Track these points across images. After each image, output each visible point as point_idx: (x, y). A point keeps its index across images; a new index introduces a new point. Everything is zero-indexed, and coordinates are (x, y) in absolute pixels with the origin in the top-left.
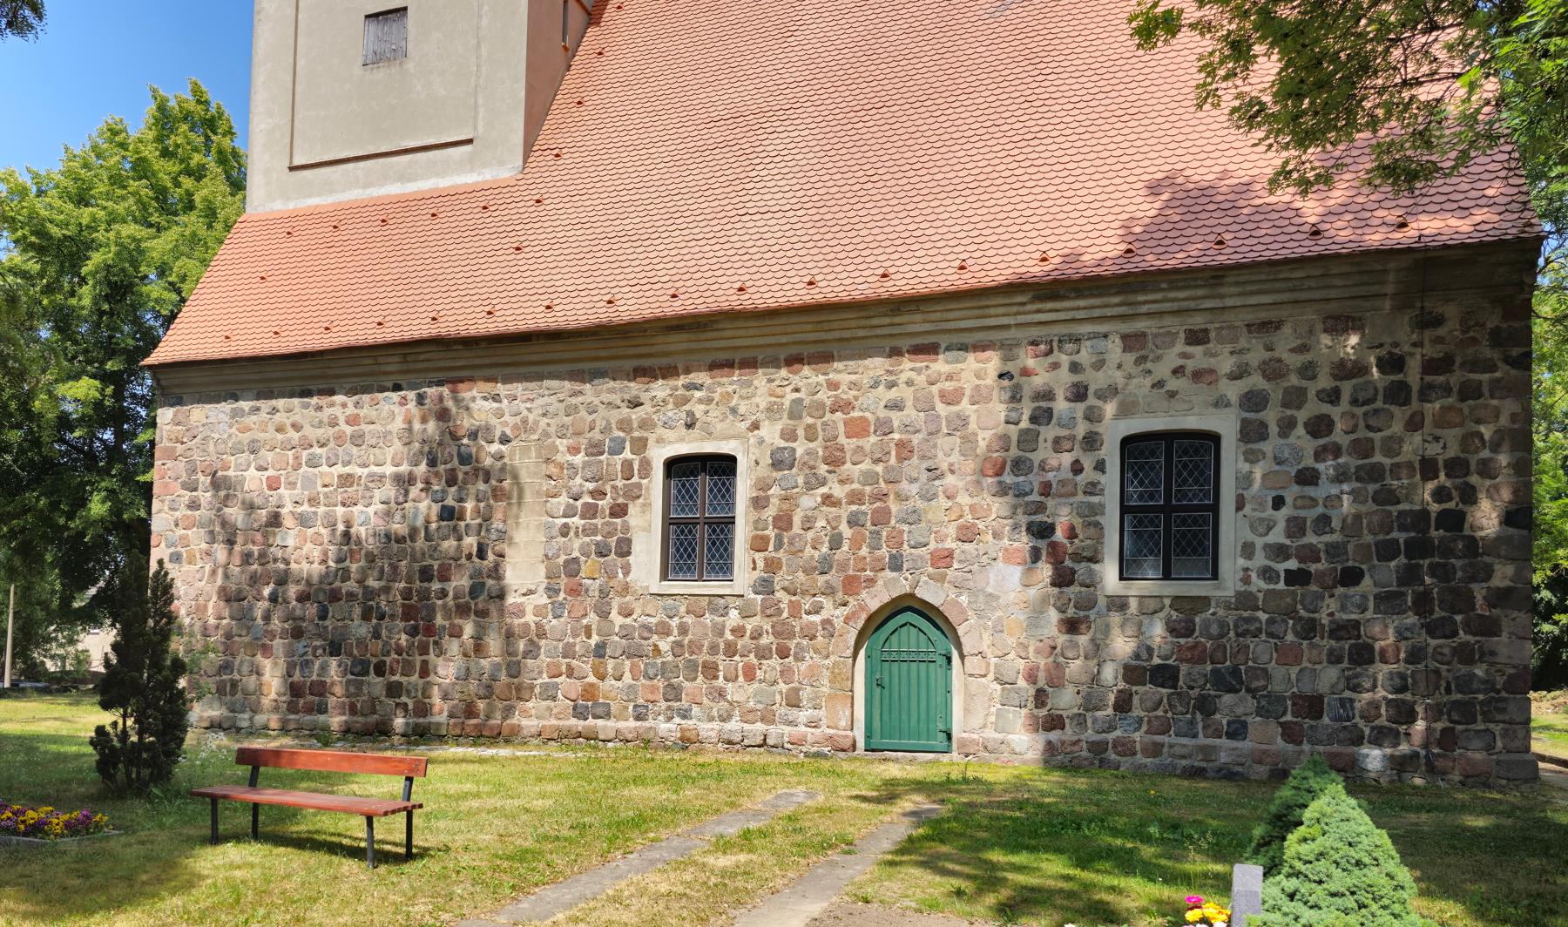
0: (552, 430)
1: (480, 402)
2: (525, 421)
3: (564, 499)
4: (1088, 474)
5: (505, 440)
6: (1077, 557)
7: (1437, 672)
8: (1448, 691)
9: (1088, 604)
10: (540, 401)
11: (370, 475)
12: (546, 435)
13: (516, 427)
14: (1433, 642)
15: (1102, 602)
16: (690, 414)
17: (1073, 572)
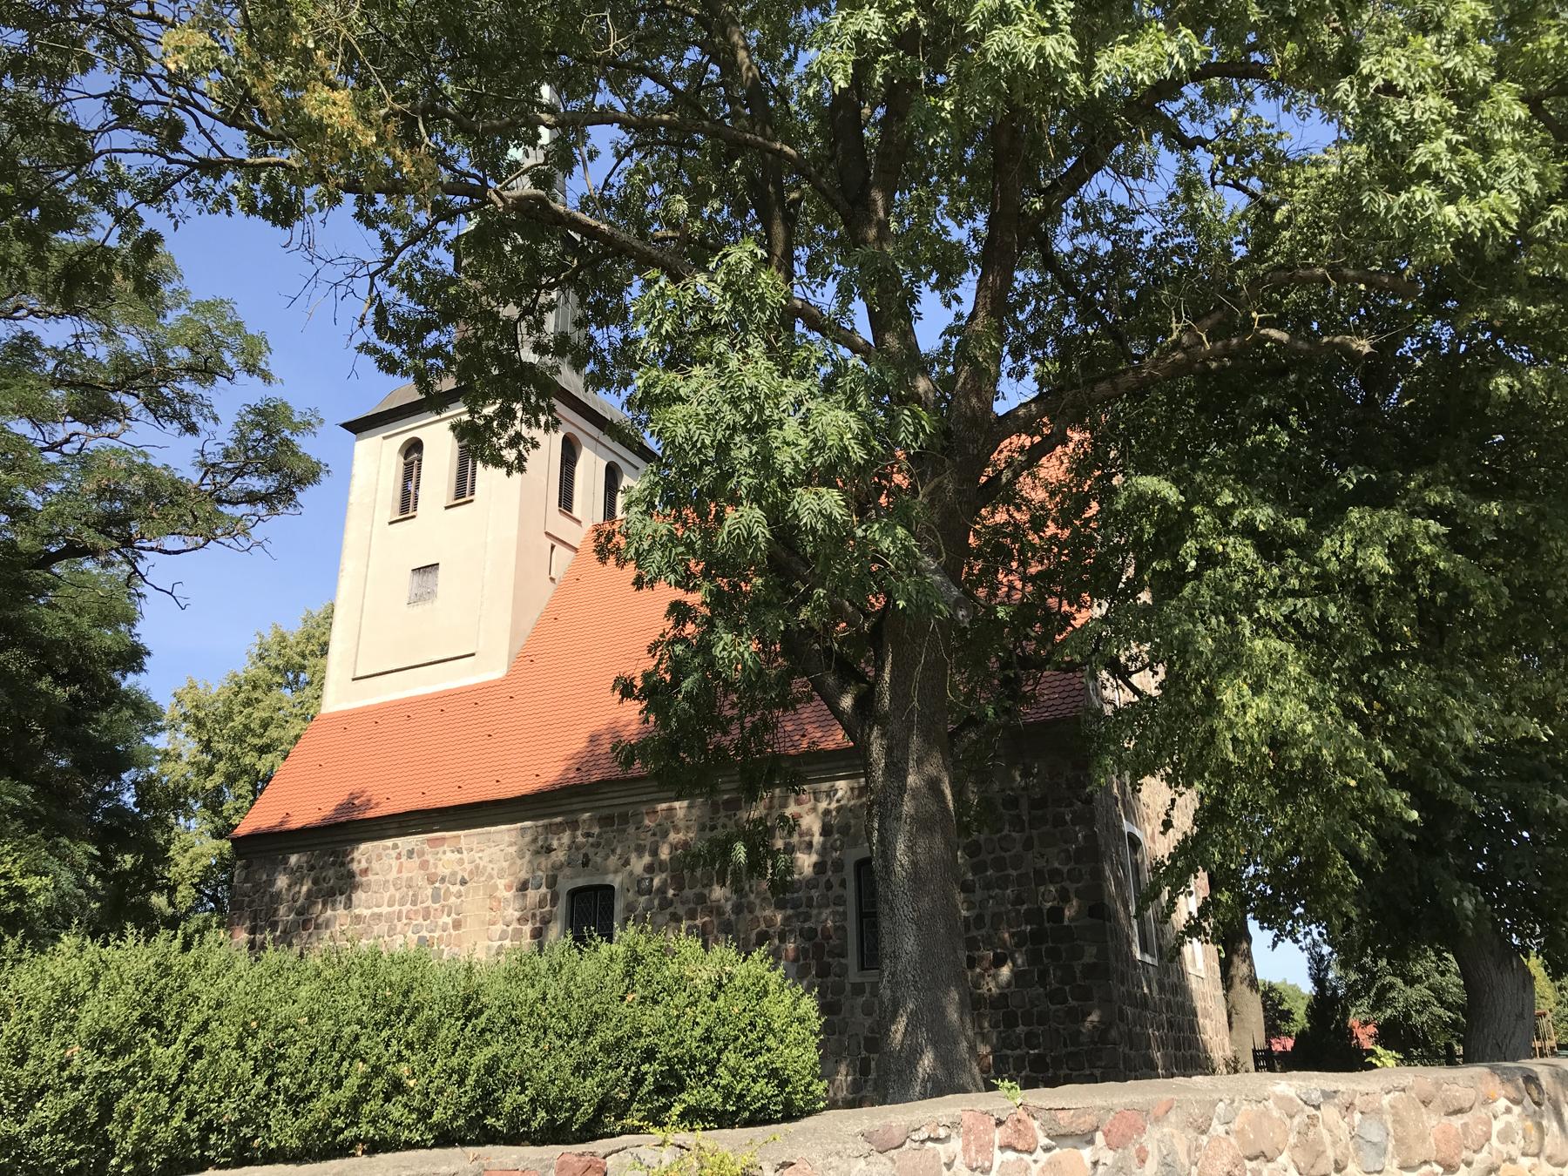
0: (495, 873)
1: (449, 854)
2: (477, 867)
3: (500, 927)
4: (837, 890)
5: (463, 882)
6: (832, 954)
7: (1057, 1030)
8: (1065, 1045)
9: (839, 990)
10: (488, 851)
11: (373, 915)
12: (491, 877)
13: (471, 872)
14: (1053, 1007)
15: (848, 987)
16: (586, 855)
17: (830, 965)
